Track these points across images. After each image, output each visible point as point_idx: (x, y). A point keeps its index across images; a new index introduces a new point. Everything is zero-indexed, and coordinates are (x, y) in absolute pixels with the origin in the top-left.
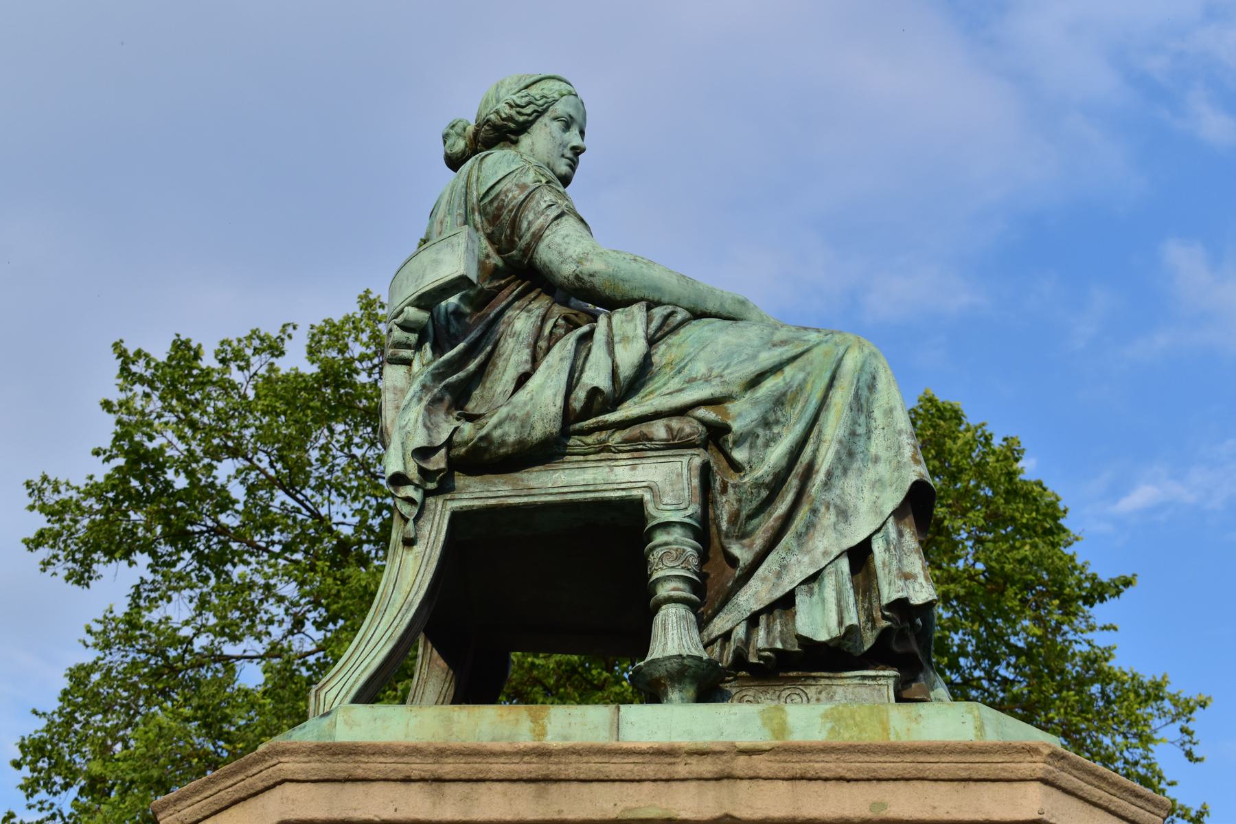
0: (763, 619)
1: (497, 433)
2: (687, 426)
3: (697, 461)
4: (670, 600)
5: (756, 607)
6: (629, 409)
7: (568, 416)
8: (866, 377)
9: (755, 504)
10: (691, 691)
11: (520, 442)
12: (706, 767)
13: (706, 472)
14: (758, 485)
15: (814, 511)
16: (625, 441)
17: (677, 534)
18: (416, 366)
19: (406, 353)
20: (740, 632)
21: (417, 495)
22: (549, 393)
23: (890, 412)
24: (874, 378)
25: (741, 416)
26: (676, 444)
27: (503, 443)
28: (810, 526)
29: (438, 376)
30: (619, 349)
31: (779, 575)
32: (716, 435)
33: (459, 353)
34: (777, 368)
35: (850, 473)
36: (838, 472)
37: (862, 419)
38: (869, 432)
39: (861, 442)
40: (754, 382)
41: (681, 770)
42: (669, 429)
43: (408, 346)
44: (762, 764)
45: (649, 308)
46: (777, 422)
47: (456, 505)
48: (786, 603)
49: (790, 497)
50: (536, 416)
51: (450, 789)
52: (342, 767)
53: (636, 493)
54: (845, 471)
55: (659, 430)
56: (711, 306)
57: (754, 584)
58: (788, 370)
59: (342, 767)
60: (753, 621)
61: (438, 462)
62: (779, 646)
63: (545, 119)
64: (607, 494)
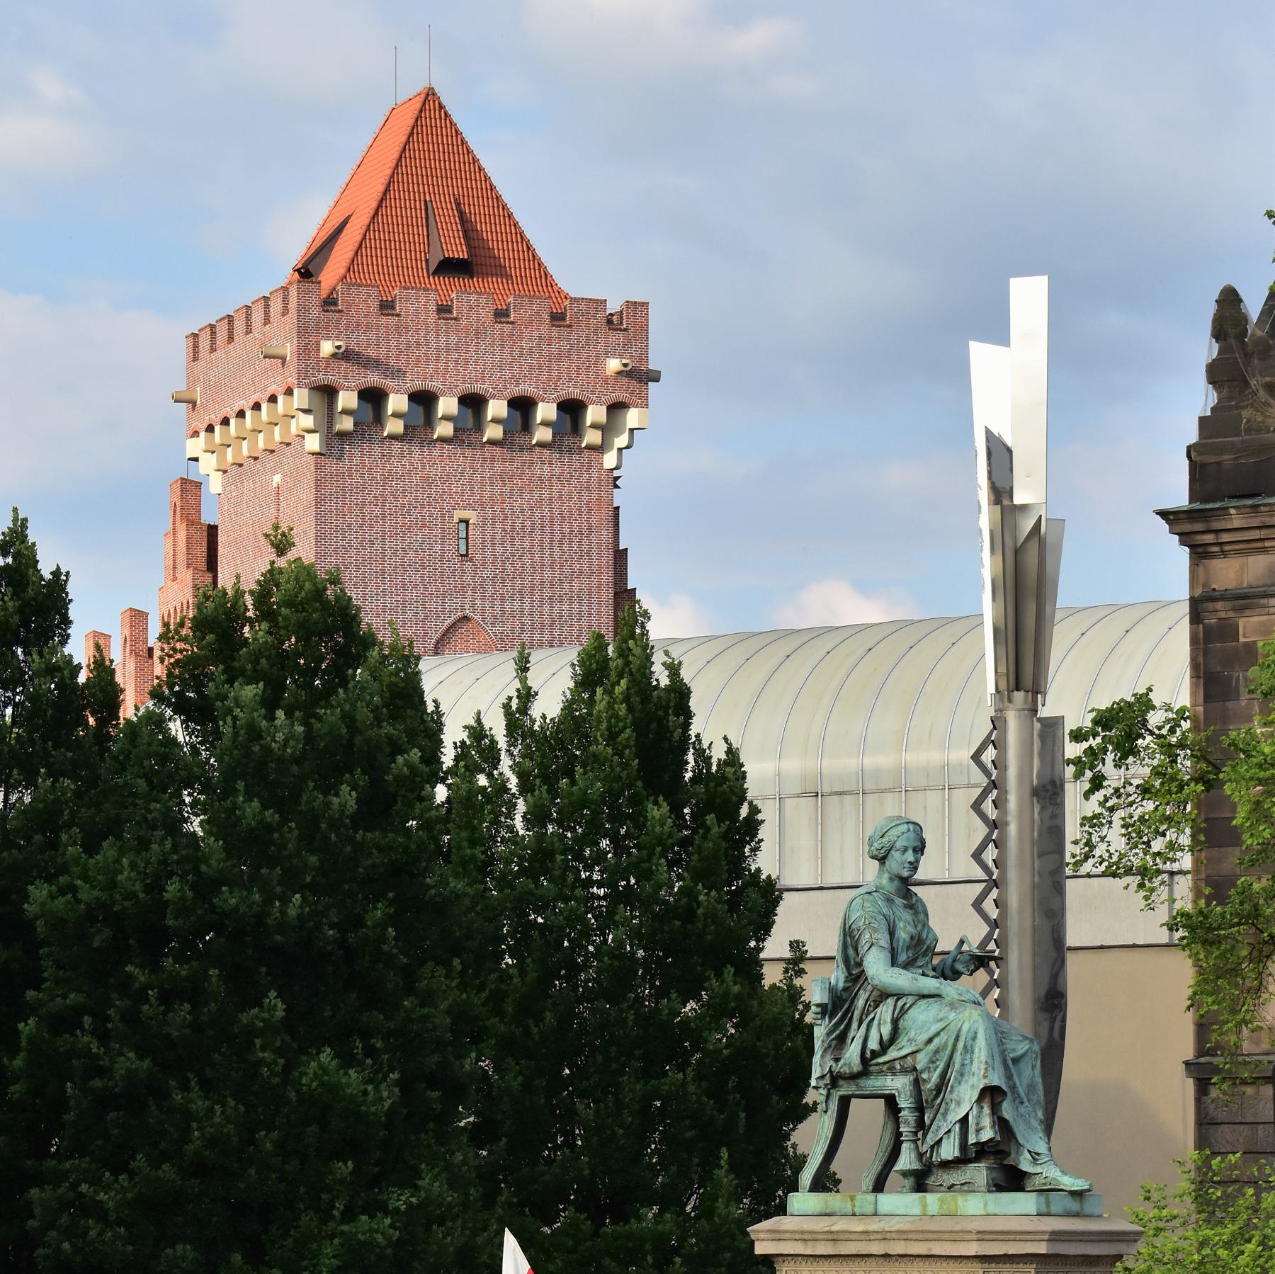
1: (842, 1070)
3: (912, 1078)
6: (892, 1054)
8: (971, 1035)
9: (932, 1096)
11: (850, 1073)
12: (879, 1236)
15: (947, 1104)
16: (888, 1069)
22: (855, 1054)
23: (980, 1049)
24: (976, 1033)
25: (921, 1061)
26: (904, 1071)
27: (846, 1073)
28: (946, 1110)
31: (937, 1131)
33: (839, 1018)
34: (938, 1034)
35: (962, 1083)
36: (956, 1084)
37: (968, 1056)
38: (971, 1062)
39: (967, 1068)
40: (930, 1041)
41: (872, 1237)
44: (895, 1236)
46: (937, 1060)
50: (852, 1064)
51: (809, 1243)
52: (777, 1236)
53: (893, 1092)
54: (960, 1083)
56: (926, 992)
57: (930, 1135)
59: (777, 1236)
61: (827, 1080)
63: (893, 852)
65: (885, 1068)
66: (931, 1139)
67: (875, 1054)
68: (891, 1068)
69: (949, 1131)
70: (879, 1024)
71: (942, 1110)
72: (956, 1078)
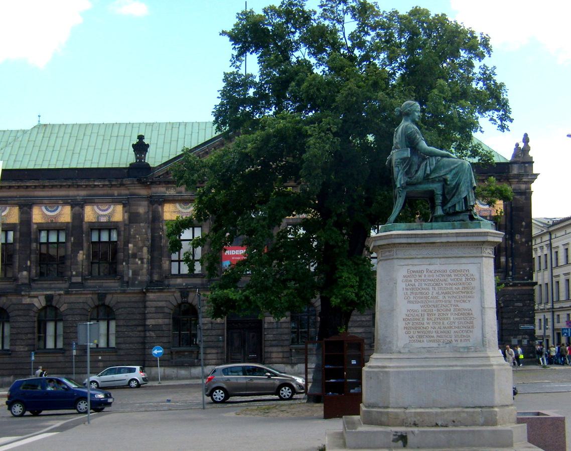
2: (441, 179)
7: (424, 177)
13: (443, 186)
18: (400, 168)
20: (448, 209)
25: (449, 177)
26: (439, 181)
29: (404, 169)
30: (431, 167)
32: (445, 180)
48: (454, 206)
57: (450, 203)
60: (450, 208)
66: (449, 205)
67: (428, 175)
68: (433, 181)
70: (430, 165)
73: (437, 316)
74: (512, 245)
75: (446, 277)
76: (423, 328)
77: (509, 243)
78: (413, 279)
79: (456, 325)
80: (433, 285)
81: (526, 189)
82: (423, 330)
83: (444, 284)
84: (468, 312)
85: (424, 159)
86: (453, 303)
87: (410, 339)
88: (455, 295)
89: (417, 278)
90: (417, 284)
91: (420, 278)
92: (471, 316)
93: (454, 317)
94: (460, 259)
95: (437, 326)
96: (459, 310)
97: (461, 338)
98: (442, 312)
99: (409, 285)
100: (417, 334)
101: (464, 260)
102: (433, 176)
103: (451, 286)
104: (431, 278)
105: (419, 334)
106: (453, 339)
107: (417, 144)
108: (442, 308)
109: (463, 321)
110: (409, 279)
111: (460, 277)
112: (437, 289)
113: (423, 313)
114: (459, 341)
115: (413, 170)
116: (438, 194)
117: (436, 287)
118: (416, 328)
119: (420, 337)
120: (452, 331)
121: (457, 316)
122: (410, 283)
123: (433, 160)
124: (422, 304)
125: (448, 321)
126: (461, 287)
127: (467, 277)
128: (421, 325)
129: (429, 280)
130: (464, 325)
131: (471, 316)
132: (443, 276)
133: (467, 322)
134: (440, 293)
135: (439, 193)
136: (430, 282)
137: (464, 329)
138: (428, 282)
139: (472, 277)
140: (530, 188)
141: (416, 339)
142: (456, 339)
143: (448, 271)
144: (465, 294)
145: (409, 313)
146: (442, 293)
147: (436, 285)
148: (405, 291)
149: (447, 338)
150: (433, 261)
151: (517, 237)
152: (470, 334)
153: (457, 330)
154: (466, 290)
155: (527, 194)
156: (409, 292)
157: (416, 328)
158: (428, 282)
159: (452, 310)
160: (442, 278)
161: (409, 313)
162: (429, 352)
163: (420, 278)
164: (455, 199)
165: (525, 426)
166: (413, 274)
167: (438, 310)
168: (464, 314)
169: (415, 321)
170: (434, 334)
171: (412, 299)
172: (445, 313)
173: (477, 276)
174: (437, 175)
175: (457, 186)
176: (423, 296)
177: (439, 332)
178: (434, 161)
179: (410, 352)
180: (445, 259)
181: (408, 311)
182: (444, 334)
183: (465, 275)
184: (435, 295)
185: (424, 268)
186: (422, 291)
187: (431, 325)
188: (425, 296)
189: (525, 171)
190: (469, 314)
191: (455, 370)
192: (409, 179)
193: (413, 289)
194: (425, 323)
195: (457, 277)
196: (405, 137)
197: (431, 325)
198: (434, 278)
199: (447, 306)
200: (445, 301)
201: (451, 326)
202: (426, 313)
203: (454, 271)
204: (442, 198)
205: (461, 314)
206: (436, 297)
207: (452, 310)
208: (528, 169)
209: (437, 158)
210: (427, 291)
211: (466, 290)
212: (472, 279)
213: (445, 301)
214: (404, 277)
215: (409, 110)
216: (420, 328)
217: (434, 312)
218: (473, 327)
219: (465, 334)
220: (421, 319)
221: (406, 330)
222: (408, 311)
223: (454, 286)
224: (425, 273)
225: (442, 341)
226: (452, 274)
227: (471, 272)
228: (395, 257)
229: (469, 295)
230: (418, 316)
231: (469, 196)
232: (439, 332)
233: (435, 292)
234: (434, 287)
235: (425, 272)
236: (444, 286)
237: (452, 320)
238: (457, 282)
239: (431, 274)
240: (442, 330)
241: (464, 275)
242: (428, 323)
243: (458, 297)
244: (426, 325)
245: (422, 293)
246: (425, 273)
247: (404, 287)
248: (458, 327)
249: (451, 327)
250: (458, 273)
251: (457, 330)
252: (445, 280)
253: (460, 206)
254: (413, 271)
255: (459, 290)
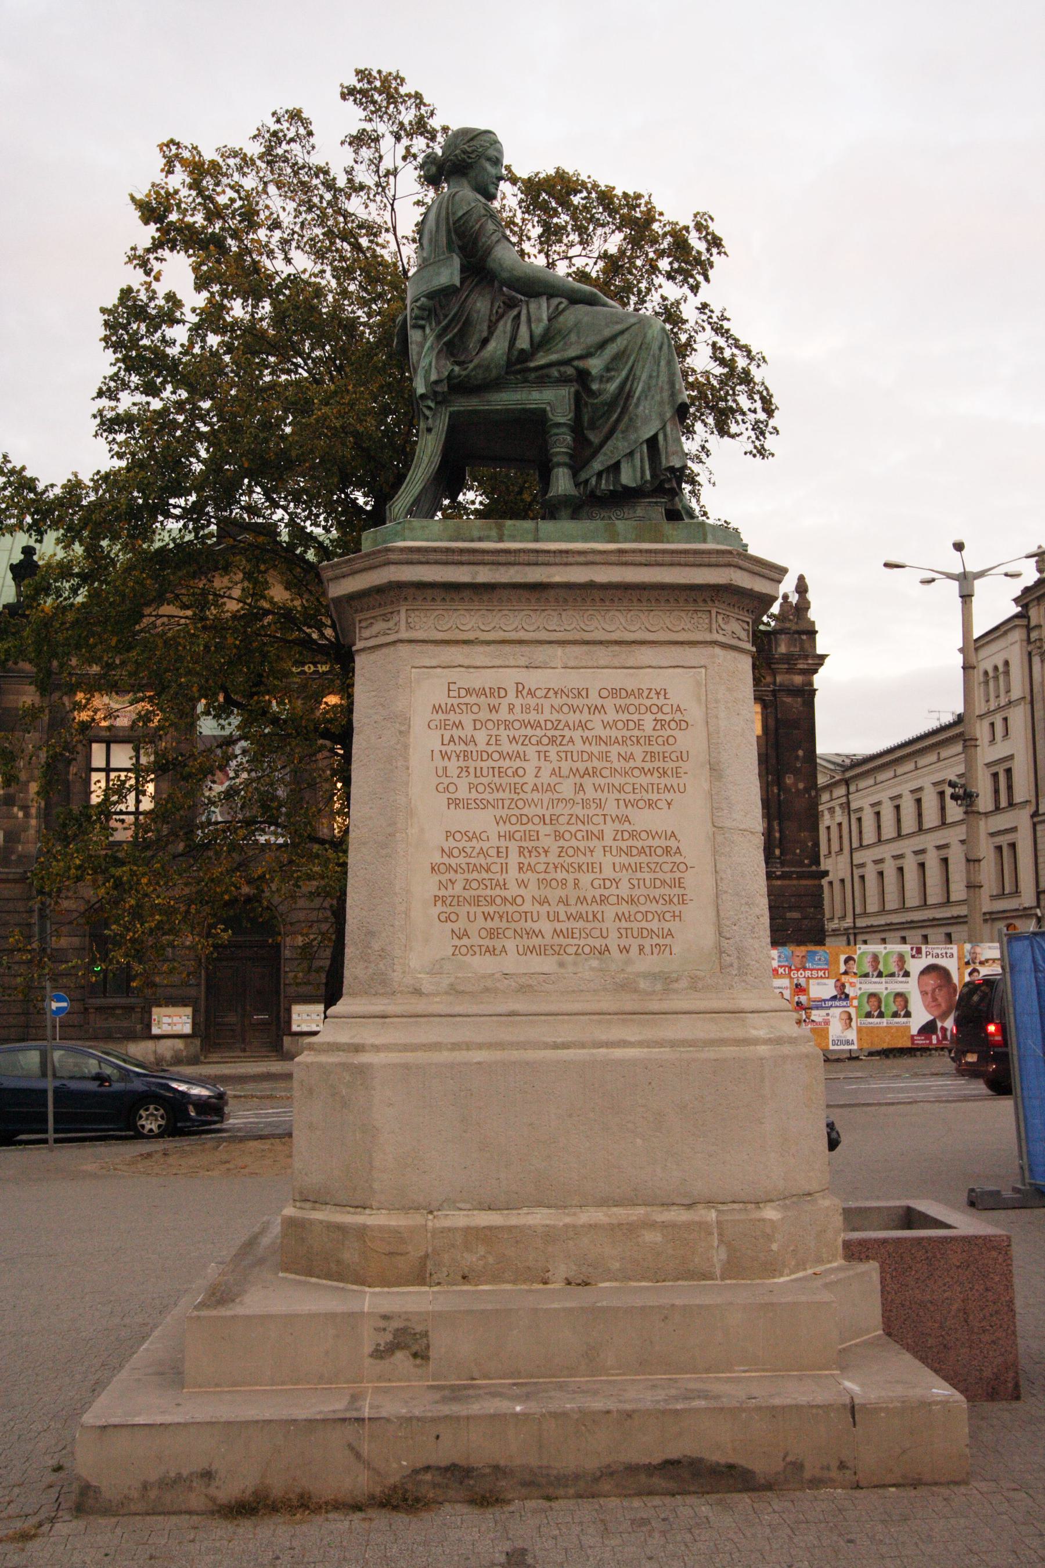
0: (604, 476)
2: (570, 371)
3: (573, 389)
4: (559, 465)
5: (601, 468)
6: (541, 360)
7: (509, 363)
10: (569, 511)
13: (578, 398)
14: (604, 404)
16: (537, 378)
17: (563, 430)
18: (428, 330)
19: (422, 322)
20: (593, 481)
21: (432, 405)
25: (595, 365)
26: (564, 380)
29: (439, 337)
30: (533, 326)
32: (583, 377)
40: (602, 345)
41: (571, 559)
42: (559, 371)
43: (423, 319)
45: (548, 299)
47: (452, 409)
48: (616, 467)
49: (619, 410)
53: (543, 406)
55: (554, 372)
57: (600, 458)
58: (619, 340)
60: (599, 474)
62: (611, 488)
64: (528, 406)
65: (533, 376)
66: (597, 465)
67: (524, 356)
68: (543, 378)
69: (631, 454)
70: (529, 321)
71: (622, 426)
72: (643, 391)
73: (552, 858)
74: (779, 795)
75: (585, 716)
76: (505, 900)
77: (772, 791)
78: (467, 720)
79: (624, 890)
80: (539, 743)
81: (804, 685)
82: (502, 909)
83: (578, 741)
84: (664, 843)
85: (511, 304)
86: (611, 809)
87: (456, 942)
88: (617, 780)
89: (484, 715)
90: (481, 737)
91: (494, 716)
92: (677, 859)
93: (617, 860)
94: (634, 648)
95: (553, 895)
96: (633, 835)
97: (640, 941)
98: (574, 843)
99: (452, 739)
100: (481, 922)
101: (646, 655)
102: (541, 360)
103: (603, 748)
104: (533, 716)
105: (489, 924)
106: (613, 942)
107: (489, 251)
108: (573, 829)
109: (648, 876)
110: (453, 717)
111: (636, 717)
112: (552, 755)
113: (503, 843)
114: (635, 950)
115: (473, 344)
116: (558, 425)
117: (552, 750)
118: (476, 901)
119: (493, 933)
120: (610, 911)
121: (624, 859)
122: (457, 733)
123: (539, 308)
124: (499, 813)
125: (591, 876)
126: (638, 751)
127: (660, 716)
128: (498, 891)
129: (525, 724)
130: (657, 893)
131: (677, 859)
132: (573, 709)
133: (663, 882)
134: (565, 772)
135: (562, 420)
136: (529, 731)
137: (653, 907)
138: (523, 731)
139: (678, 716)
140: (811, 684)
141: (481, 942)
142: (623, 942)
143: (593, 694)
144: (654, 780)
145: (451, 843)
146: (574, 772)
147: (552, 741)
148: (440, 763)
149: (590, 941)
150: (542, 654)
151: (789, 780)
152: (673, 925)
153: (624, 908)
154: (656, 764)
155: (808, 694)
156: (453, 766)
157: (476, 901)
158: (523, 731)
159: (609, 835)
160: (573, 718)
161: (451, 843)
162: (524, 989)
163: (494, 716)
164: (617, 446)
165: (871, 1269)
166: (467, 700)
167: (559, 836)
168: (651, 851)
169: (475, 875)
170: (546, 927)
171: (463, 793)
172: (582, 845)
173: (695, 713)
174: (554, 357)
175: (624, 396)
176: (505, 781)
177: (563, 917)
178: (541, 310)
179: (454, 991)
180: (585, 648)
181: (449, 834)
182: (581, 924)
183: (655, 709)
184: (545, 777)
185: (509, 678)
186: (501, 763)
187: (533, 889)
188: (513, 780)
189: (802, 649)
190: (667, 851)
191: (620, 1062)
192: (457, 369)
193: (466, 755)
194: (512, 884)
195: (625, 716)
196: (449, 232)
197: (533, 889)
198: (541, 718)
199: (590, 819)
200: (585, 804)
201: (606, 893)
202: (513, 846)
203: (614, 693)
204: (574, 440)
205: (642, 851)
206: (551, 788)
207: (609, 835)
208: (807, 645)
209: (555, 301)
210: (518, 763)
211: (656, 764)
212: (678, 723)
213: (585, 804)
214: (436, 709)
215: (464, 152)
216: (493, 902)
217: (546, 842)
218: (682, 900)
219: (655, 925)
220: (494, 868)
221: (439, 908)
222: (449, 834)
223: (615, 749)
224: (511, 697)
225: (571, 950)
226: (609, 704)
227: (674, 700)
228: (404, 635)
229: (663, 781)
230: (486, 855)
231: (665, 436)
232: (563, 917)
233: (547, 768)
234: (540, 748)
235: (512, 693)
236: (579, 745)
237: (608, 872)
238: (625, 732)
239: (532, 702)
240: (573, 910)
241: (649, 709)
242: (522, 884)
243: (628, 788)
244: (513, 890)
245: (501, 772)
246: (511, 697)
247: (438, 747)
248: (632, 901)
249: (604, 900)
250: (628, 701)
251: (624, 908)
252: (583, 726)
253: (634, 466)
254: (468, 691)
255: (632, 764)
